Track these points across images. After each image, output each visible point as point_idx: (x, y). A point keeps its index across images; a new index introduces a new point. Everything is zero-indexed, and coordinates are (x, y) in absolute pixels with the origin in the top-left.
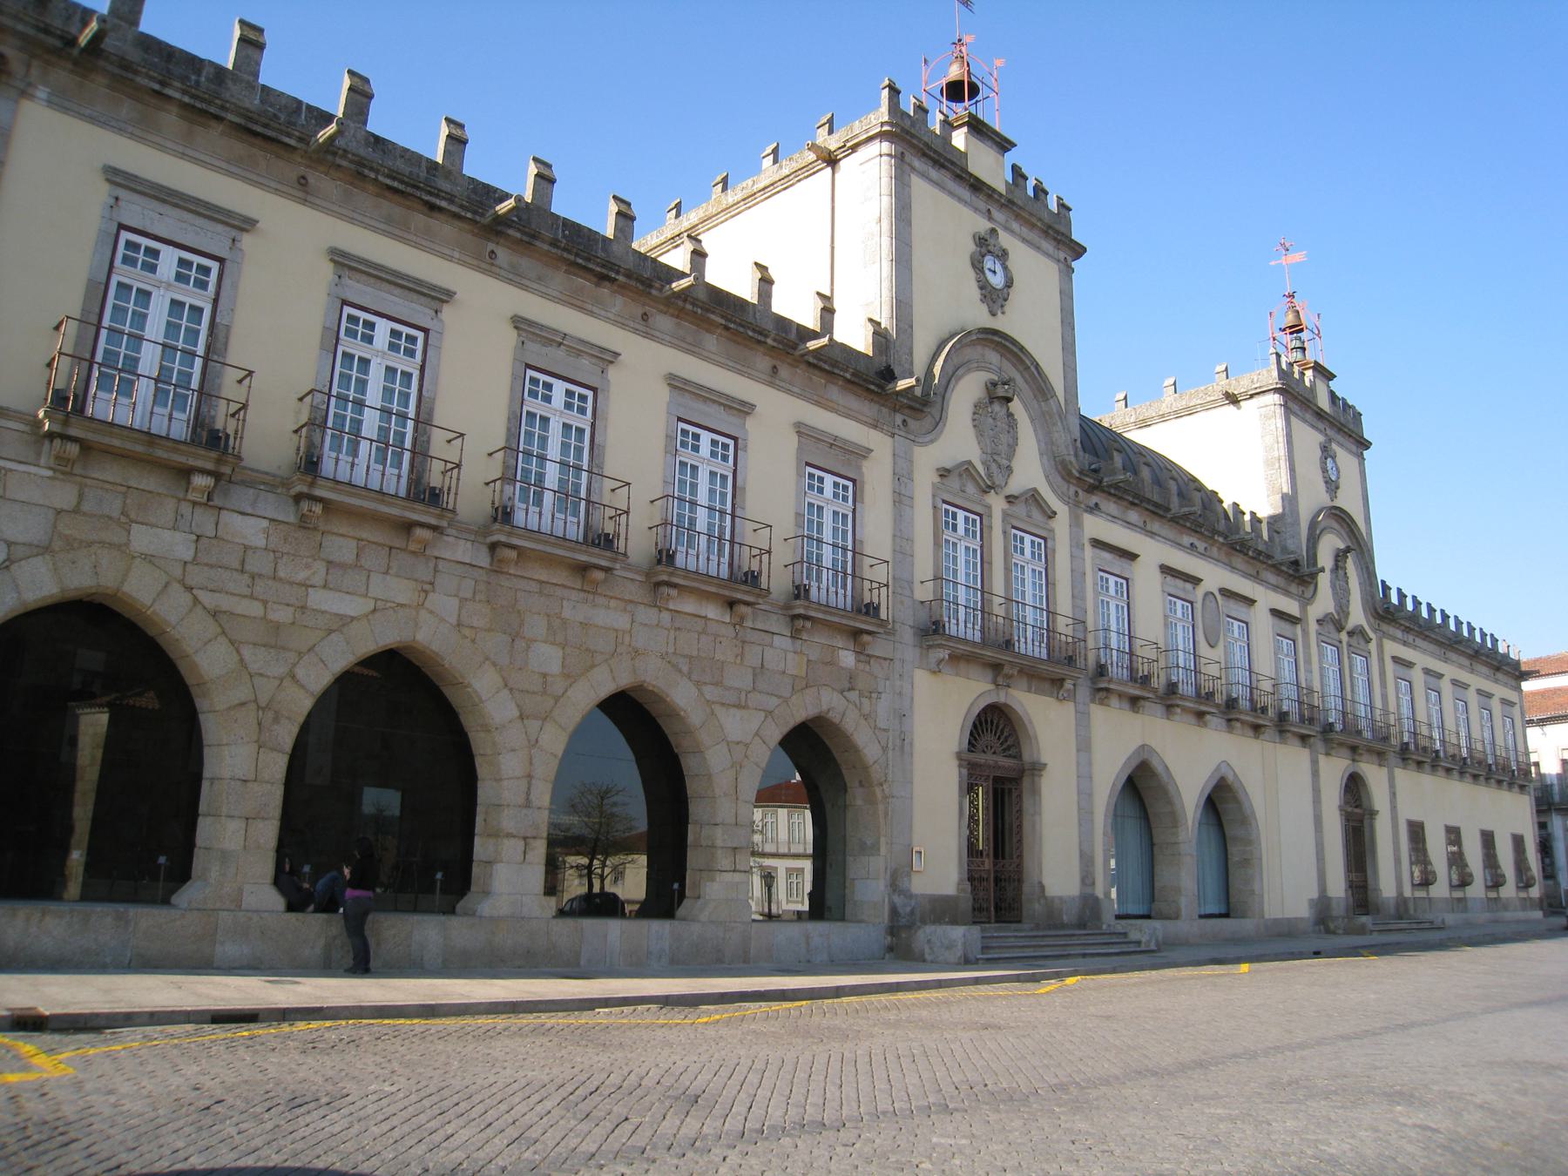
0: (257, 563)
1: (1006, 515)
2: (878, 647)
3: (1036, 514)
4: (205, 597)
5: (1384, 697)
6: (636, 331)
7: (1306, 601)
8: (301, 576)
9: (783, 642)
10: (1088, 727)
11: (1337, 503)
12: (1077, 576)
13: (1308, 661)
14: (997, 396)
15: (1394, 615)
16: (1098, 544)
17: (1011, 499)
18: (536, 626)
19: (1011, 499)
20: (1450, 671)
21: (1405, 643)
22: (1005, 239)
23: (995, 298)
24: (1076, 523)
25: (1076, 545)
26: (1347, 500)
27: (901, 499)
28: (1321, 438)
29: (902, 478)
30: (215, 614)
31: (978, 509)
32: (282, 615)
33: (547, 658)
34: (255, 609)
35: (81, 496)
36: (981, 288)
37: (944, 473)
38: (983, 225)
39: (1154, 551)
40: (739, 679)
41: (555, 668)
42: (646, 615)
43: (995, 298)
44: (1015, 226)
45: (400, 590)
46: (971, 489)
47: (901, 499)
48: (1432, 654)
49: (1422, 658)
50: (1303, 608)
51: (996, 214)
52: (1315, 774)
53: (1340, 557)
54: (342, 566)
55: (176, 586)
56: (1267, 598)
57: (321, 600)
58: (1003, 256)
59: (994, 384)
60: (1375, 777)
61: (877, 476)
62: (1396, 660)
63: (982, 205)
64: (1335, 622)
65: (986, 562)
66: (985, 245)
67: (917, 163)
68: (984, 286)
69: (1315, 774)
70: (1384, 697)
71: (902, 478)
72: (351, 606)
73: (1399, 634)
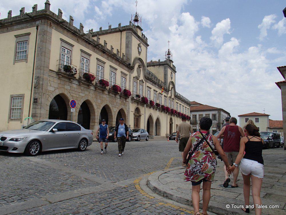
0: (76, 90)
1: (139, 83)
2: (127, 100)
3: (142, 83)
4: (71, 94)
5: (175, 107)
6: (107, 59)
7: (168, 94)
8: (79, 91)
9: (119, 99)
10: (145, 110)
11: (172, 81)
12: (145, 91)
13: (167, 102)
14: (139, 67)
15: (178, 97)
16: (148, 86)
17: (140, 81)
18: (98, 98)
19: (140, 81)
20: (183, 104)
21: (178, 100)
22: (141, 45)
23: (139, 53)
24: (146, 84)
25: (145, 87)
26: (173, 80)
27: (130, 81)
28: (171, 71)
29: (130, 78)
30: (72, 96)
31: (137, 82)
32: (78, 96)
33: (99, 101)
34: (75, 95)
35: (60, 82)
36: (138, 52)
37: (134, 77)
38: (139, 42)
39: (153, 88)
40: (115, 104)
41: (100, 103)
42: (107, 96)
43: (139, 53)
44: (143, 43)
45: (87, 93)
46: (136, 79)
47: (130, 81)
48: (180, 102)
49: (180, 102)
50: (167, 95)
51: (141, 41)
52: (167, 117)
53: (172, 88)
54: (82, 90)
55: (69, 93)
56: (164, 94)
57: (81, 94)
58: (141, 47)
59: (139, 65)
60: (173, 118)
61: (128, 77)
62: (176, 102)
63: (139, 39)
64: (170, 97)
65: (137, 89)
66: (139, 45)
67: (133, 34)
68: (139, 51)
69: (167, 117)
70: (175, 107)
71: (130, 78)
72: (83, 95)
73: (177, 99)
